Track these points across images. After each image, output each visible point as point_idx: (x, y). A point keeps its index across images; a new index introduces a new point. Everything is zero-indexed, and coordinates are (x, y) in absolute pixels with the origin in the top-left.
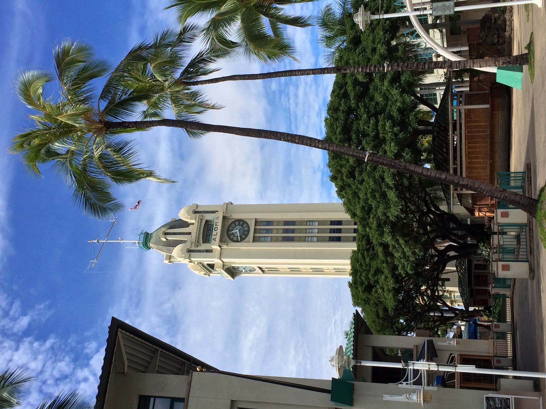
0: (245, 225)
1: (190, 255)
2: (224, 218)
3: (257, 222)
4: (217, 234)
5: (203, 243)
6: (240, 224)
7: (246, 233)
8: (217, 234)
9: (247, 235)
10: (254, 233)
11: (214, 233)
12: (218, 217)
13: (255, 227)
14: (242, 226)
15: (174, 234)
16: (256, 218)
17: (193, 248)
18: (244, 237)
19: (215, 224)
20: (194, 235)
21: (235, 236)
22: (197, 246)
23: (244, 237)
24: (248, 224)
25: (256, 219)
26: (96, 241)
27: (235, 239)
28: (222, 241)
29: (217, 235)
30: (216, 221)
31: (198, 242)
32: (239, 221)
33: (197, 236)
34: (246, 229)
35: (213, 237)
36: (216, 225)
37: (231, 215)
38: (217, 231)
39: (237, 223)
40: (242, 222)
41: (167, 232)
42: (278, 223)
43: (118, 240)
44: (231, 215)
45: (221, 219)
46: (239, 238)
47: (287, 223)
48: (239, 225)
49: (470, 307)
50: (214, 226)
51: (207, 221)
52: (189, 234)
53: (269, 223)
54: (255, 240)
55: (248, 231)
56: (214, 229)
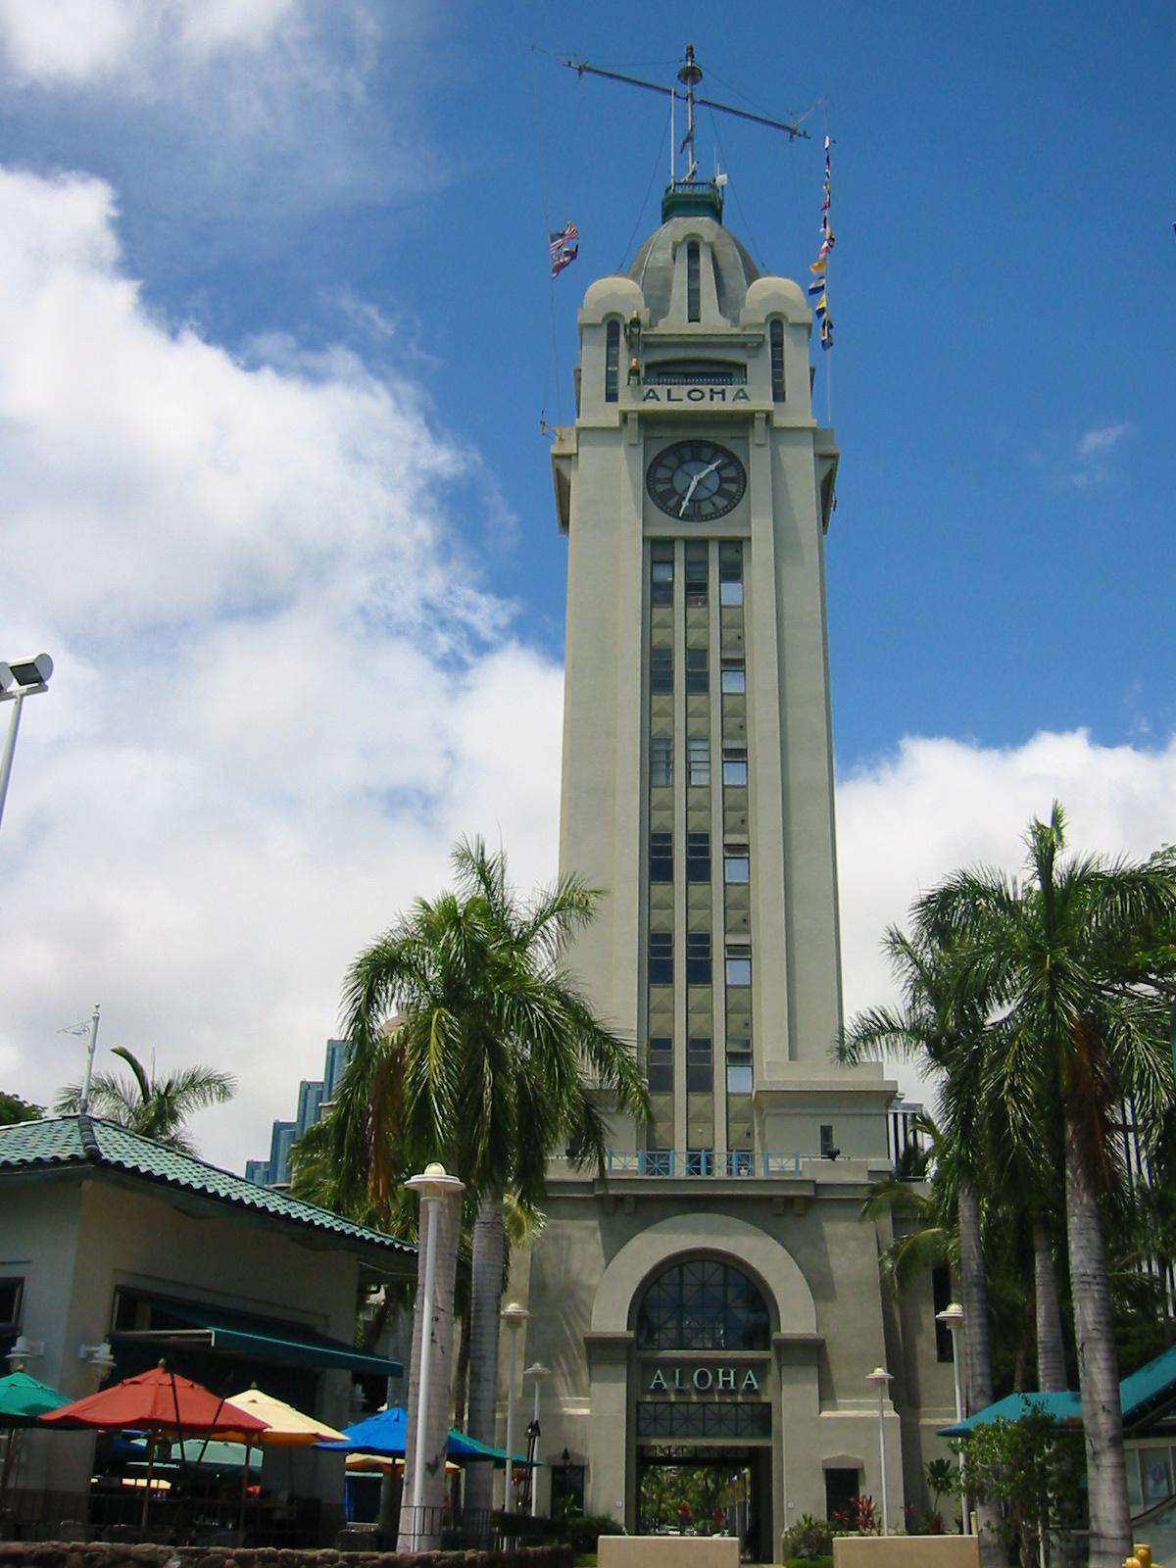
0: (721, 502)
4: (675, 398)
6: (725, 486)
8: (675, 398)
9: (673, 512)
10: (690, 543)
11: (681, 391)
12: (746, 397)
13: (713, 539)
14: (720, 492)
24: (725, 513)
25: (750, 539)
27: (662, 473)
28: (648, 421)
29: (669, 399)
30: (731, 390)
32: (742, 480)
36: (711, 390)
38: (686, 399)
39: (728, 473)
40: (733, 487)
45: (741, 406)
48: (722, 480)
50: (706, 389)
51: (742, 368)
54: (658, 550)
56: (692, 387)
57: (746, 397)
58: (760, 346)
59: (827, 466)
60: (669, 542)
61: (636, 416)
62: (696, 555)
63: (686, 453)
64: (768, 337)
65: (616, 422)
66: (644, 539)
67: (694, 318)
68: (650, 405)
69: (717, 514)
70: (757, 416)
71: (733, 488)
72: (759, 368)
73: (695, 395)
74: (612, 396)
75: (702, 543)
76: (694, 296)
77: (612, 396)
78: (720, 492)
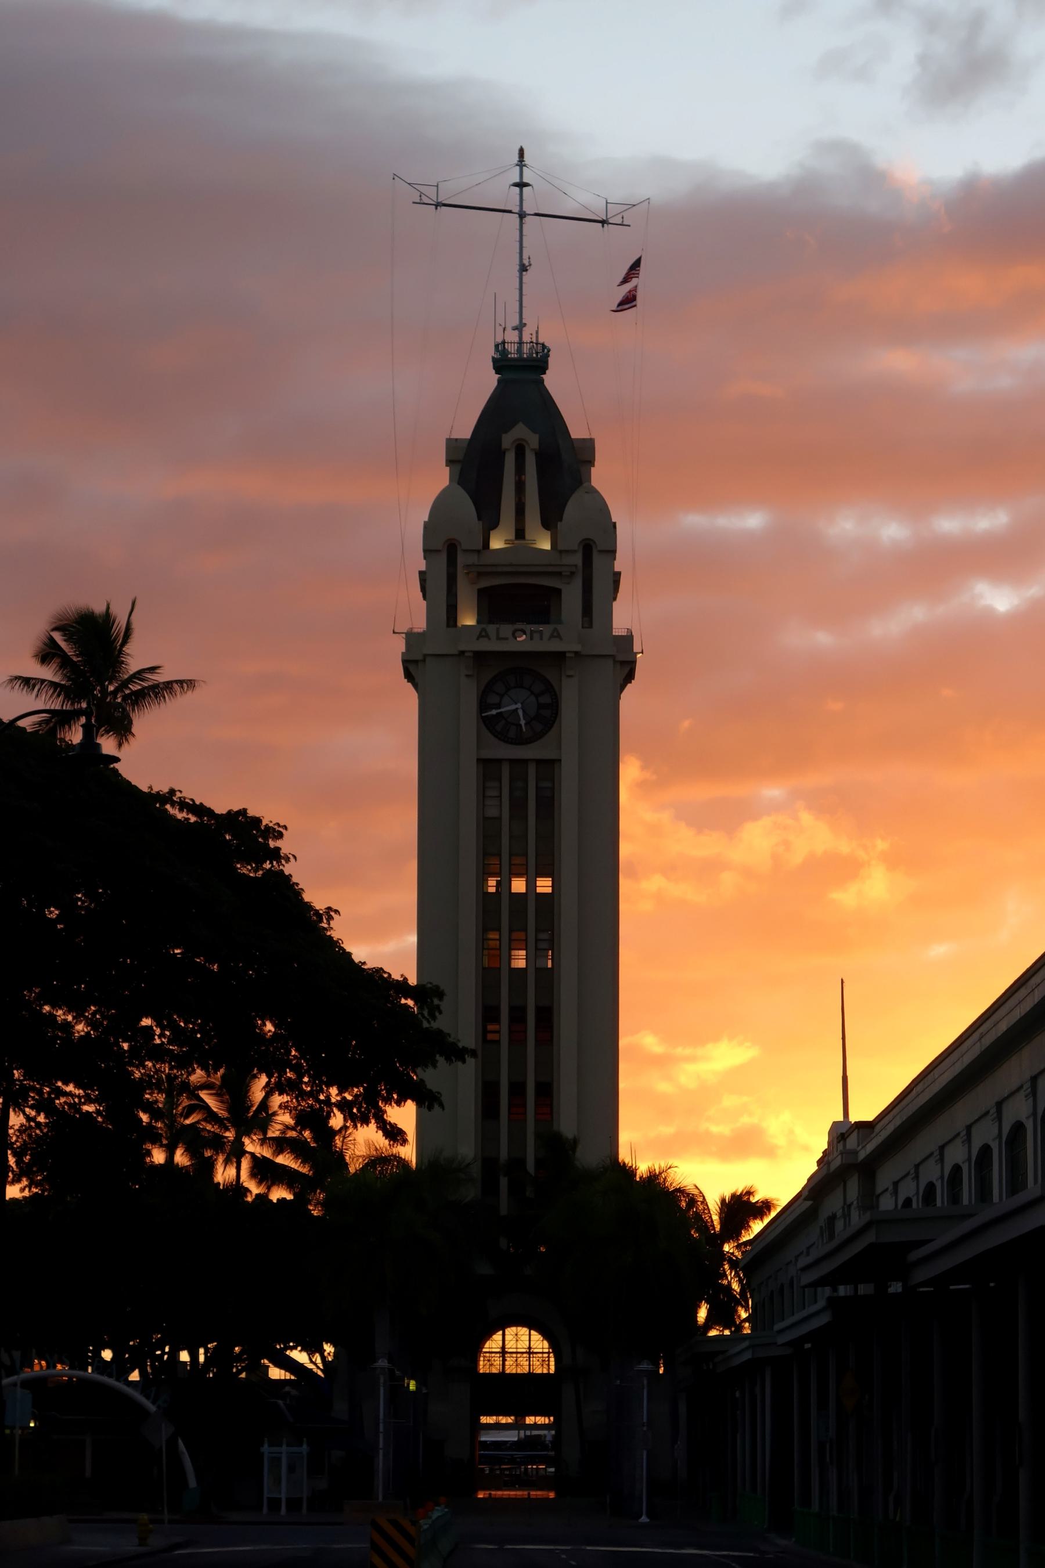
1: (438, 551)
3: (549, 767)
9: (503, 737)
10: (512, 761)
12: (559, 637)
16: (562, 761)
17: (461, 559)
21: (502, 696)
25: (560, 760)
31: (480, 575)
32: (555, 707)
33: (500, 569)
35: (491, 629)
37: (571, 676)
39: (545, 699)
44: (571, 676)
45: (555, 646)
46: (494, 712)
51: (558, 592)
54: (488, 767)
55: (520, 740)
56: (519, 626)
57: (559, 637)
58: (572, 573)
59: (626, 670)
61: (471, 654)
64: (580, 563)
66: (478, 760)
69: (535, 737)
70: (568, 655)
75: (525, 762)
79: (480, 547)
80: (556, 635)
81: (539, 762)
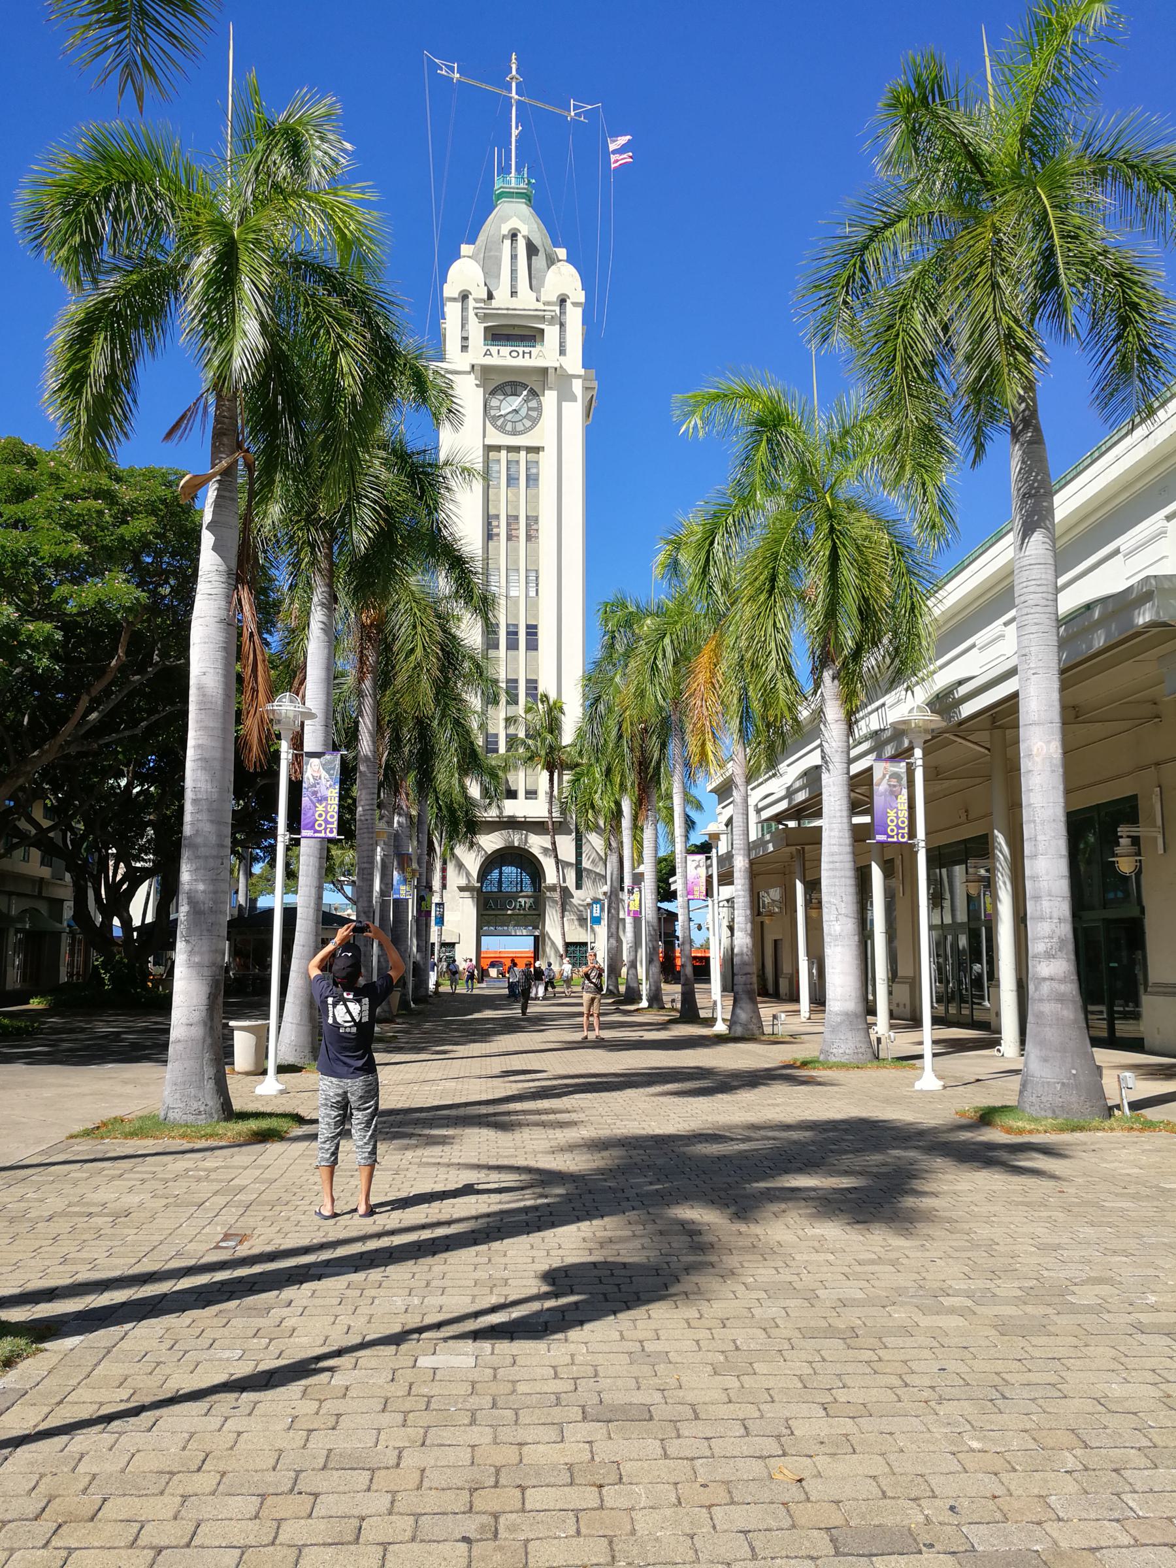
0: (528, 423)
2: (545, 371)
4: (505, 356)
5: (486, 328)
7: (509, 427)
8: (505, 356)
9: (501, 429)
11: (505, 350)
14: (527, 416)
15: (514, 257)
17: (471, 303)
18: (499, 423)
19: (527, 350)
20: (515, 303)
22: (476, 315)
23: (499, 423)
26: (514, 72)
32: (539, 409)
34: (519, 427)
35: (494, 349)
41: (520, 237)
42: (533, 501)
43: (517, 128)
47: (532, 520)
48: (529, 409)
49: (8, 988)
50: (520, 349)
52: (514, 293)
53: (532, 480)
55: (514, 433)
60: (498, 448)
62: (513, 456)
63: (508, 389)
65: (468, 369)
67: (514, 293)
68: (488, 361)
71: (534, 414)
72: (551, 333)
73: (514, 354)
74: (464, 348)
76: (514, 271)
77: (464, 348)
78: (527, 416)
79: (485, 296)
80: (541, 355)
81: (530, 450)
